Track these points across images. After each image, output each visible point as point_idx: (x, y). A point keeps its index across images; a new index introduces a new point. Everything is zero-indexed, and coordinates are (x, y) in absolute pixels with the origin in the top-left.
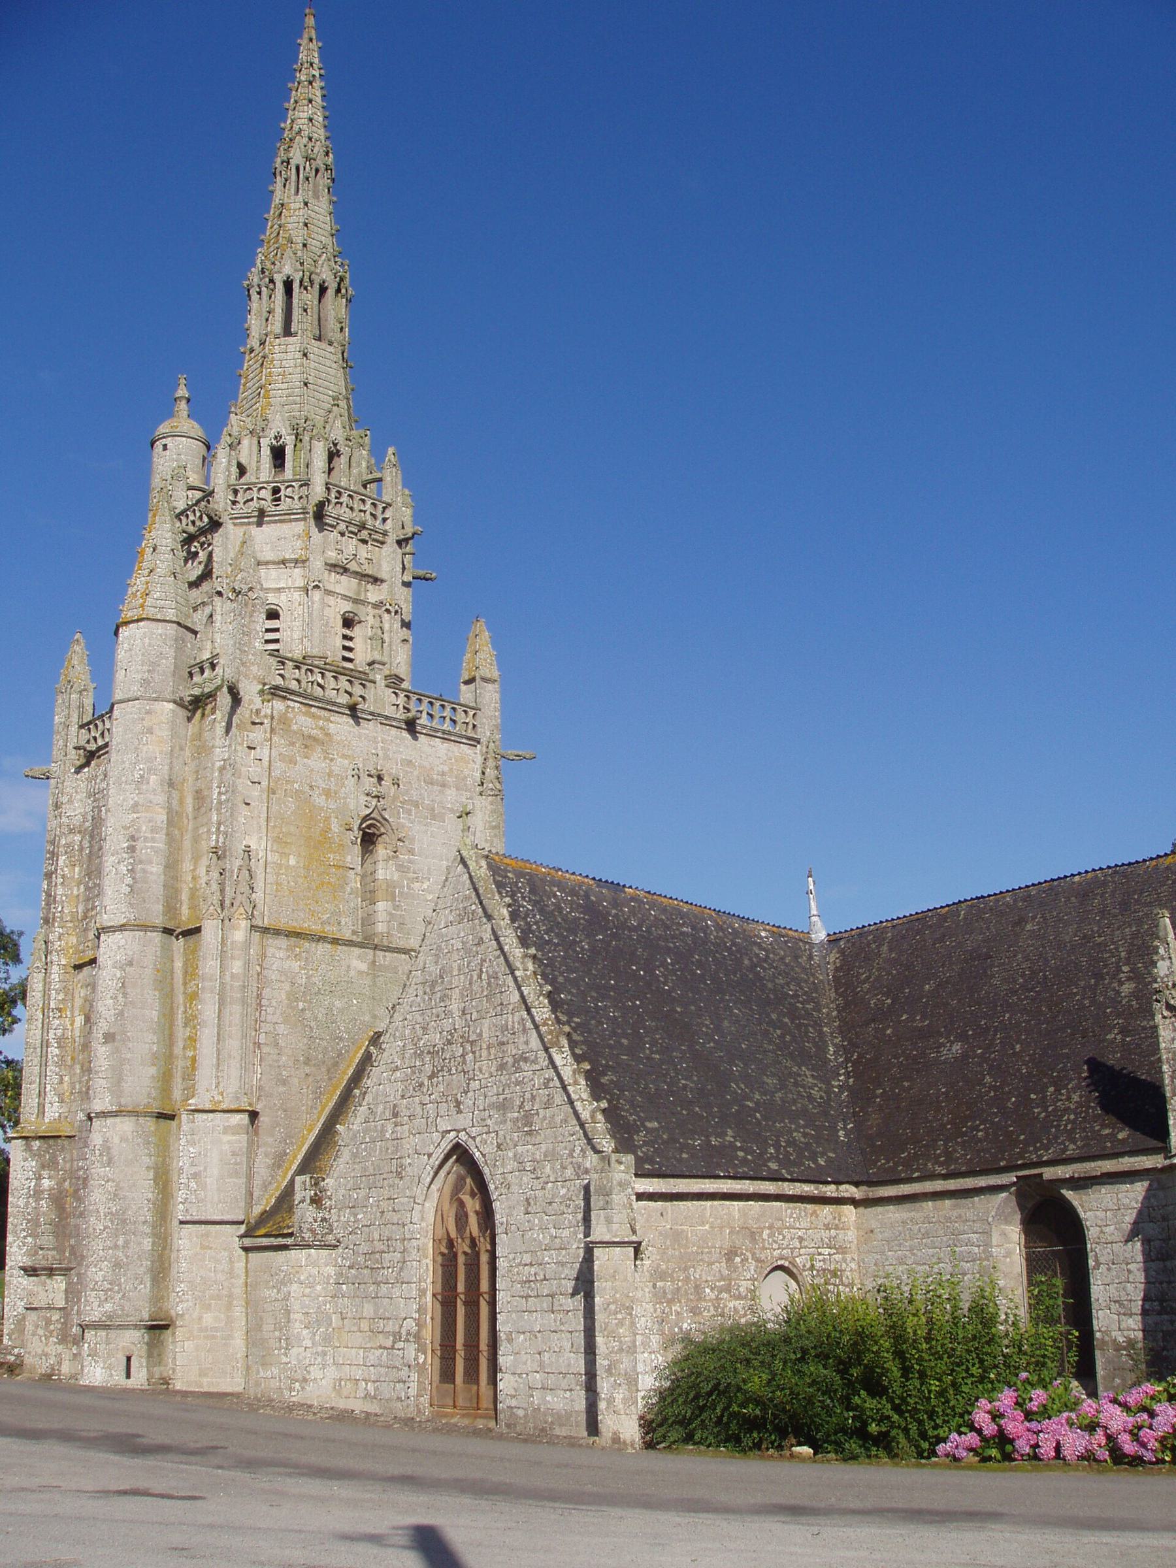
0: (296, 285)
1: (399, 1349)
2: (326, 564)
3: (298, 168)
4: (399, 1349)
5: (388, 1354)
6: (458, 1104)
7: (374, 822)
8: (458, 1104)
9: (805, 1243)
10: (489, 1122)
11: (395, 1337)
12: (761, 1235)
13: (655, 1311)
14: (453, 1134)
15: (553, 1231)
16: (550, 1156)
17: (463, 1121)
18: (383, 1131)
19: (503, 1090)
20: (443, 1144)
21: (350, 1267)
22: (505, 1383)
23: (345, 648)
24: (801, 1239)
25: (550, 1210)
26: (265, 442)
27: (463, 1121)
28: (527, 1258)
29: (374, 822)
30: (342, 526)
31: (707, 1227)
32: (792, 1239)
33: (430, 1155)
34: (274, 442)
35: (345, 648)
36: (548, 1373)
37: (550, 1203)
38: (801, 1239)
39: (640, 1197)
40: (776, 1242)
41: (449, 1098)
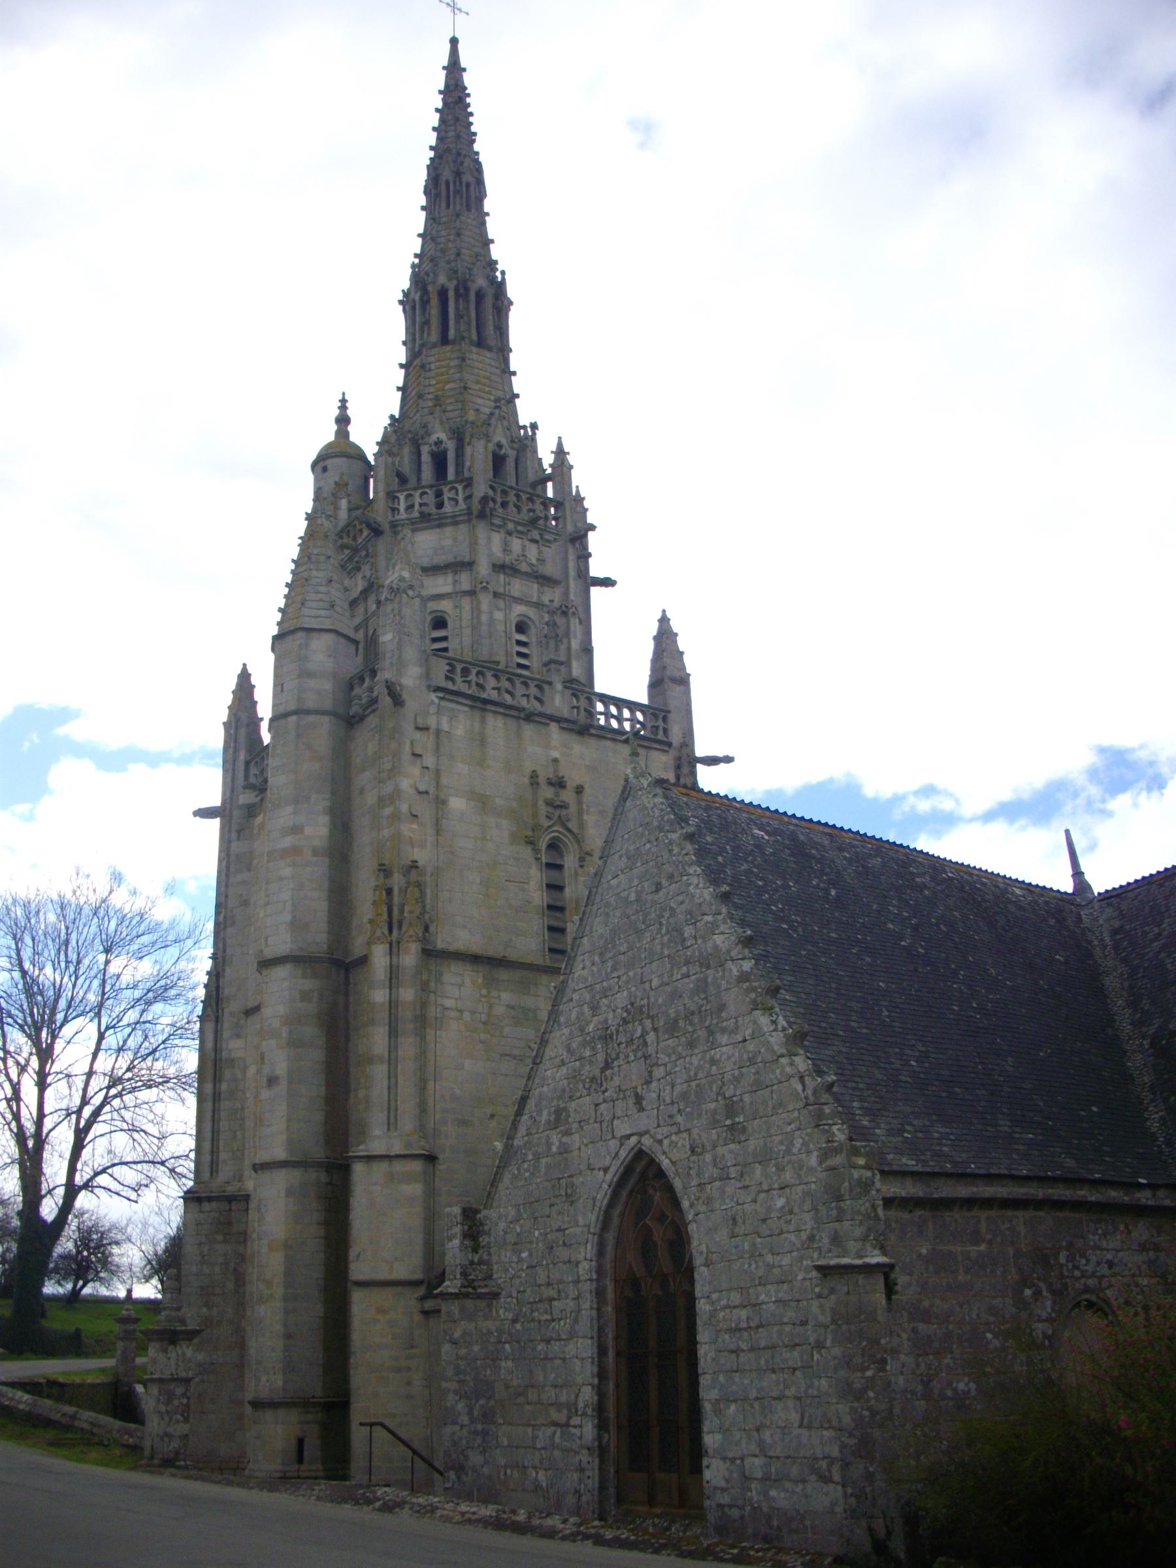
0: (451, 294)
1: (575, 1427)
2: (494, 566)
3: (448, 183)
4: (575, 1427)
5: (563, 1434)
6: (639, 1100)
7: (556, 834)
8: (639, 1100)
9: (1116, 1269)
10: (679, 1119)
11: (569, 1410)
12: (1056, 1258)
13: (918, 1365)
14: (634, 1140)
15: (769, 1258)
16: (764, 1157)
17: (645, 1121)
18: (549, 1145)
19: (696, 1074)
20: (623, 1153)
21: (514, 1321)
22: (714, 1472)
23: (520, 655)
24: (1111, 1264)
25: (764, 1229)
26: (425, 450)
27: (645, 1121)
28: (735, 1298)
29: (556, 834)
30: (510, 526)
31: (983, 1247)
32: (1098, 1263)
33: (606, 1170)
34: (435, 448)
35: (520, 655)
36: (771, 1457)
37: (764, 1220)
38: (1111, 1264)
39: (888, 1202)
40: (1077, 1268)
41: (628, 1093)
